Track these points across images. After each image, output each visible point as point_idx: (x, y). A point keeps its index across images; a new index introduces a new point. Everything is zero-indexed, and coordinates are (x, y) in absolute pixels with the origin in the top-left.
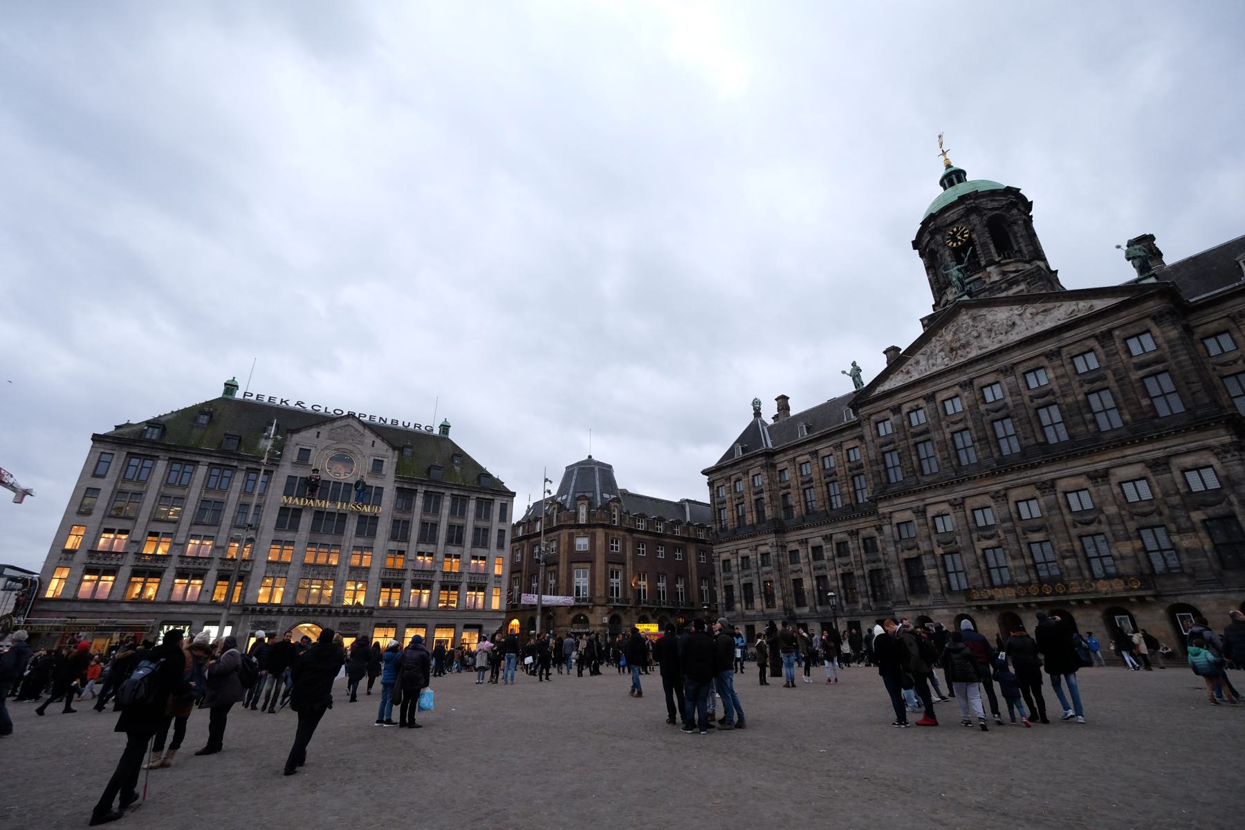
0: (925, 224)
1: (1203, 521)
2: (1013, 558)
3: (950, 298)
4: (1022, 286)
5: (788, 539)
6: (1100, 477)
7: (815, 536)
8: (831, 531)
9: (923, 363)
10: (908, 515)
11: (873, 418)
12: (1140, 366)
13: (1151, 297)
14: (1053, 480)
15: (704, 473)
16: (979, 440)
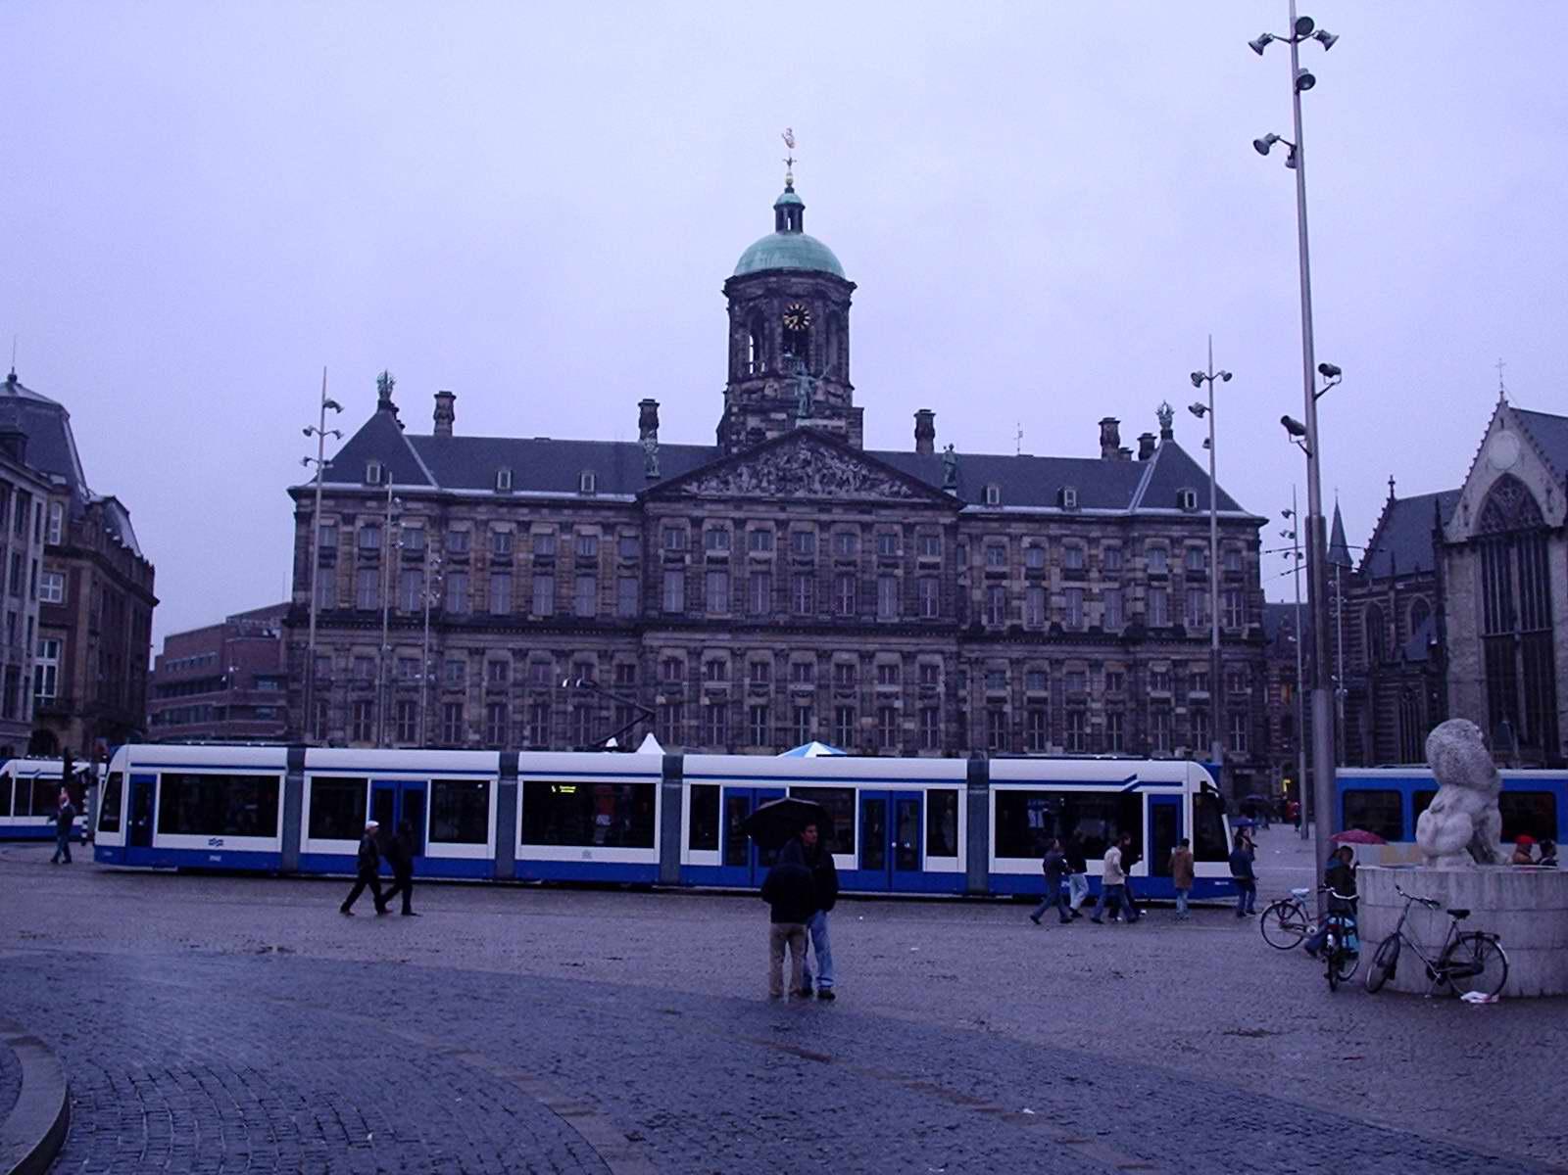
0: (766, 273)
1: (921, 710)
2: (778, 718)
3: (767, 391)
4: (842, 423)
5: (450, 643)
6: (867, 657)
7: (500, 647)
8: (529, 645)
9: (745, 477)
10: (680, 654)
11: (664, 521)
12: (923, 566)
13: (950, 508)
14: (833, 650)
15: (296, 493)
16: (778, 591)
